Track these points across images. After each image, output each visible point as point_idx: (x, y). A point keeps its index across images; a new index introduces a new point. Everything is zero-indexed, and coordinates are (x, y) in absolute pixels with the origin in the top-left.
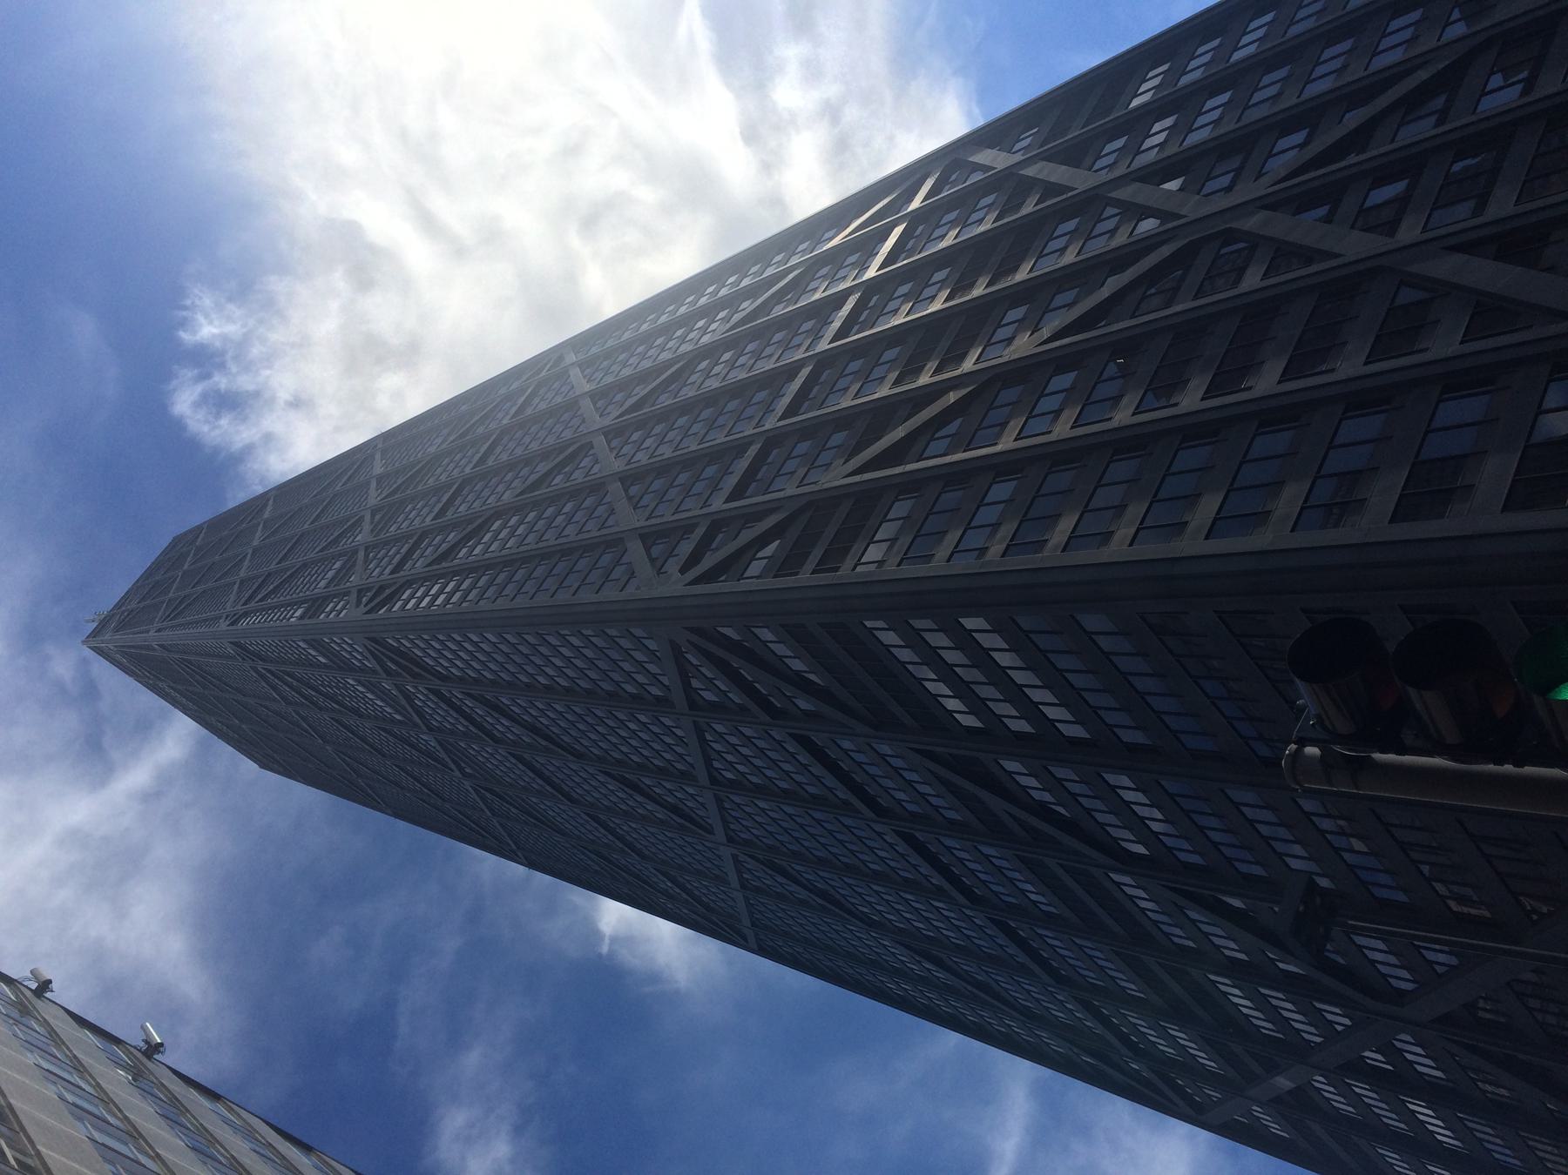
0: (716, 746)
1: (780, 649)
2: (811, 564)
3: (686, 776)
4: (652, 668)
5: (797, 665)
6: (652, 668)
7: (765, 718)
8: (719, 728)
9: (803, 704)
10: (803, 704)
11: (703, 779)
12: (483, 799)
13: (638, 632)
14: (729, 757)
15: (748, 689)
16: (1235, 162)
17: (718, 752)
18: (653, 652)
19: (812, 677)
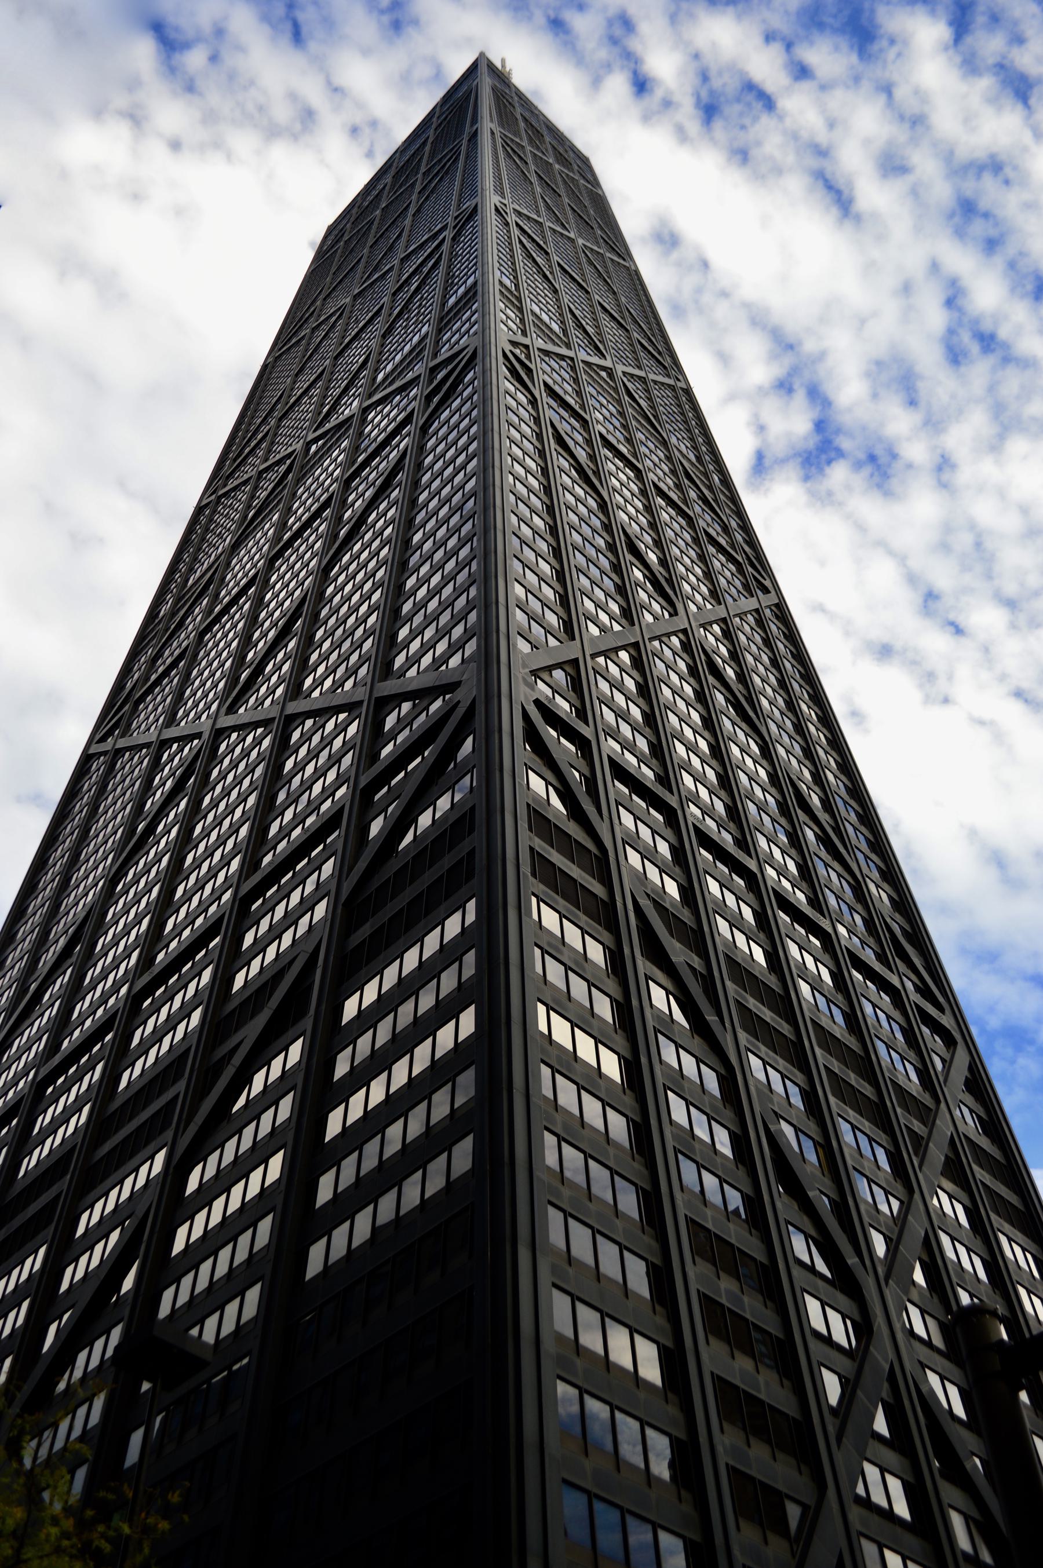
0: (330, 726)
1: (444, 803)
2: (539, 844)
3: (295, 690)
5: (425, 820)
7: (363, 781)
8: (352, 729)
9: (376, 827)
10: (376, 827)
11: (293, 708)
12: (279, 463)
14: (316, 739)
15: (400, 761)
16: (938, 1341)
17: (323, 726)
19: (409, 838)
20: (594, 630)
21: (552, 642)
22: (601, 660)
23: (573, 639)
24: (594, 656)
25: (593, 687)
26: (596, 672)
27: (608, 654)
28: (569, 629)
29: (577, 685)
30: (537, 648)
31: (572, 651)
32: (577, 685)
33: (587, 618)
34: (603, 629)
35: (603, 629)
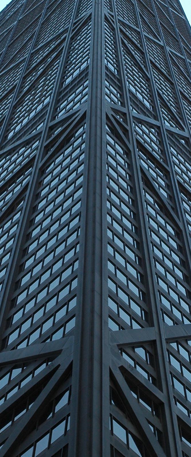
4: (35, 336)
6: (35, 336)
13: (75, 284)
18: (50, 337)
20: (169, 322)
21: (136, 326)
22: (174, 345)
23: (152, 325)
24: (169, 341)
25: (167, 364)
26: (170, 353)
27: (179, 340)
28: (149, 318)
29: (154, 359)
30: (123, 329)
31: (151, 334)
32: (154, 359)
33: (163, 312)
34: (176, 322)
35: (176, 322)
